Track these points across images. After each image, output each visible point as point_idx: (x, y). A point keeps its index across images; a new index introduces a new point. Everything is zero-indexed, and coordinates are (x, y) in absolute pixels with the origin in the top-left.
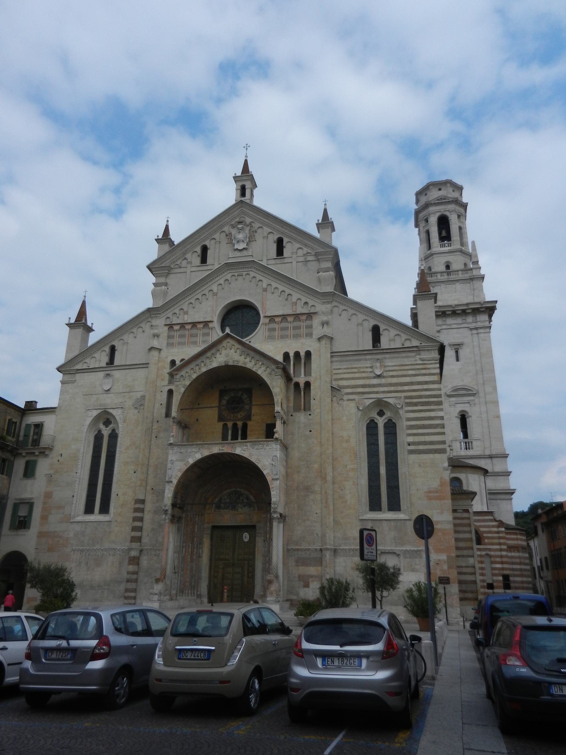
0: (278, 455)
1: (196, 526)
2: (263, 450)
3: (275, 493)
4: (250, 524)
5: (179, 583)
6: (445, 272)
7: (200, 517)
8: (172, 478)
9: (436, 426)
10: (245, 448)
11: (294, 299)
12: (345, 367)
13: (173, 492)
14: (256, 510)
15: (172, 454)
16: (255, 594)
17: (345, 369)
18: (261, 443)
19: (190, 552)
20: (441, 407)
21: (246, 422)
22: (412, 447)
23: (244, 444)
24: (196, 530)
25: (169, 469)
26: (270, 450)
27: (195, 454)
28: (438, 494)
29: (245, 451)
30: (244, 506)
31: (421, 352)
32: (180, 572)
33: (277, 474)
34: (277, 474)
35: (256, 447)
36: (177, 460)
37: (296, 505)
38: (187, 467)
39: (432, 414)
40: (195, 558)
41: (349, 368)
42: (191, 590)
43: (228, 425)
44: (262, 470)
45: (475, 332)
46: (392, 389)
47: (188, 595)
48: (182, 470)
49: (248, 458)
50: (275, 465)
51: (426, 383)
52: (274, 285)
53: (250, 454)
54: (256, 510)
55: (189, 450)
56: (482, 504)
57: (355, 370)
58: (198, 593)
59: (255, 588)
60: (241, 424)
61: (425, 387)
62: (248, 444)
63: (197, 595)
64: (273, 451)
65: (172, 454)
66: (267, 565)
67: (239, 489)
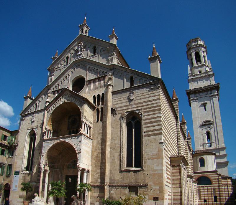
6: (199, 74)
9: (158, 121)
11: (98, 71)
12: (118, 98)
17: (118, 99)
20: (160, 111)
22: (146, 134)
28: (156, 156)
31: (152, 86)
39: (156, 116)
41: (119, 99)
45: (211, 97)
46: (138, 105)
51: (154, 100)
52: (91, 67)
56: (213, 168)
57: (122, 99)
61: (153, 102)
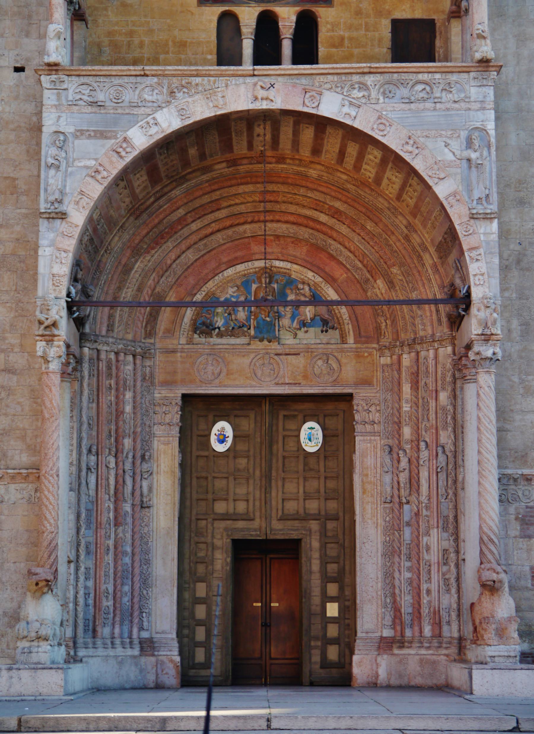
0: (491, 126)
1: (129, 395)
2: (429, 105)
3: (484, 270)
4: (330, 390)
5: (81, 601)
7: (138, 362)
8: (66, 201)
10: (356, 94)
13: (71, 255)
14: (351, 340)
15: (56, 107)
16: (359, 634)
18: (420, 77)
19: (112, 492)
21: (314, 9)
23: (356, 78)
24: (128, 408)
25: (49, 167)
26: (456, 106)
27: (157, 111)
29: (359, 107)
30: (303, 324)
32: (82, 557)
33: (487, 196)
34: (487, 196)
35: (404, 92)
36: (80, 133)
37: (515, 323)
38: (124, 163)
42: (121, 624)
43: (241, 20)
44: (430, 182)
47: (112, 643)
48: (105, 174)
49: (370, 133)
50: (479, 166)
53: (379, 118)
54: (351, 340)
55: (128, 96)
58: (145, 635)
59: (358, 613)
60: (294, 18)
62: (369, 80)
63: (141, 642)
64: (470, 109)
65: (56, 107)
66: (407, 533)
67: (277, 263)
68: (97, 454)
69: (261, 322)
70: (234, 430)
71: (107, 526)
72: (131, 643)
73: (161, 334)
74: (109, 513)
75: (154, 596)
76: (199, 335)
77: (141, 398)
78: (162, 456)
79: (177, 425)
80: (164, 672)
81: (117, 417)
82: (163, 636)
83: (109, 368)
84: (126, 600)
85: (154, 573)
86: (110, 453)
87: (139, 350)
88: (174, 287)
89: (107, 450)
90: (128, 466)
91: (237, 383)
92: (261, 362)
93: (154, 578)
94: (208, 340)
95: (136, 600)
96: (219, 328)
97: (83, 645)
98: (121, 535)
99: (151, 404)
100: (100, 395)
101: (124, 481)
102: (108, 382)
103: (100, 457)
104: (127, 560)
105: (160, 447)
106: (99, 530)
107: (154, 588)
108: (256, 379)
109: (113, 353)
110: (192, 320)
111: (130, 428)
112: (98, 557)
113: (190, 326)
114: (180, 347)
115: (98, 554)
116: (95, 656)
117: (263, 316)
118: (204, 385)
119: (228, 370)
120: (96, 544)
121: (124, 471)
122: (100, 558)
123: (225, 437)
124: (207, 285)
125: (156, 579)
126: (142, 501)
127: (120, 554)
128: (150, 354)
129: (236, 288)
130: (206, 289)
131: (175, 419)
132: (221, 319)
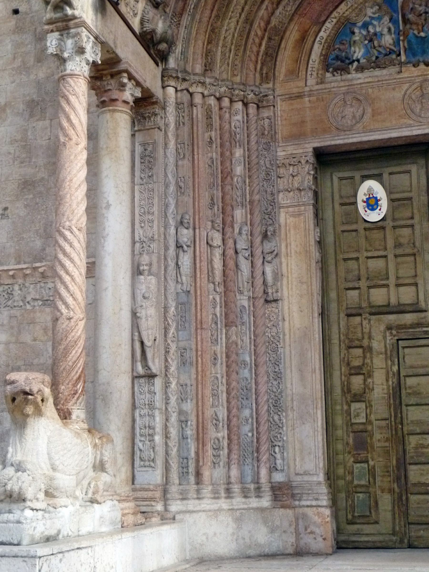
1: (238, 153)
5: (174, 432)
24: (239, 170)
40: (246, 304)
42: (241, 464)
58: (278, 477)
68: (194, 229)
69: (413, 40)
70: (389, 192)
71: (213, 325)
72: (258, 489)
73: (282, 77)
74: (214, 308)
75: (290, 423)
76: (332, 73)
77: (257, 157)
78: (292, 232)
79: (310, 189)
80: (309, 530)
81: (223, 180)
82: (306, 478)
83: (209, 117)
84: (246, 429)
85: (289, 392)
86: (213, 227)
87: (251, 96)
88: (296, 18)
89: (210, 223)
90: (242, 245)
91: (388, 124)
92: (418, 93)
93: (289, 398)
94: (344, 77)
95: (263, 428)
96: (358, 60)
97: (177, 496)
98: (234, 338)
99: (272, 165)
100: (196, 150)
101: (237, 266)
102: (207, 135)
103: (197, 231)
104: (246, 373)
105: (288, 221)
106: (199, 331)
107: (289, 412)
108: (412, 115)
109: (213, 97)
110: (321, 54)
111: (244, 195)
112: (200, 369)
113: (319, 63)
114: (307, 89)
115: (200, 365)
116: (200, 511)
117: (416, 32)
118: (343, 133)
119: (373, 110)
120: (197, 350)
121: (236, 252)
122: (203, 371)
123: (377, 200)
124: (339, 10)
125: (292, 400)
126: (265, 292)
127: (234, 365)
128: (268, 101)
129: (377, 7)
130: (337, 15)
131: (306, 182)
132: (360, 49)
